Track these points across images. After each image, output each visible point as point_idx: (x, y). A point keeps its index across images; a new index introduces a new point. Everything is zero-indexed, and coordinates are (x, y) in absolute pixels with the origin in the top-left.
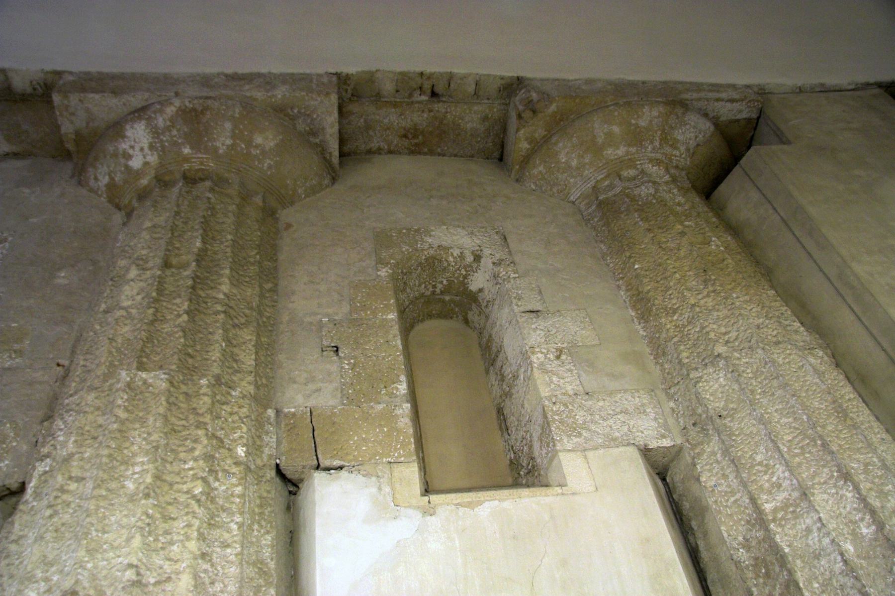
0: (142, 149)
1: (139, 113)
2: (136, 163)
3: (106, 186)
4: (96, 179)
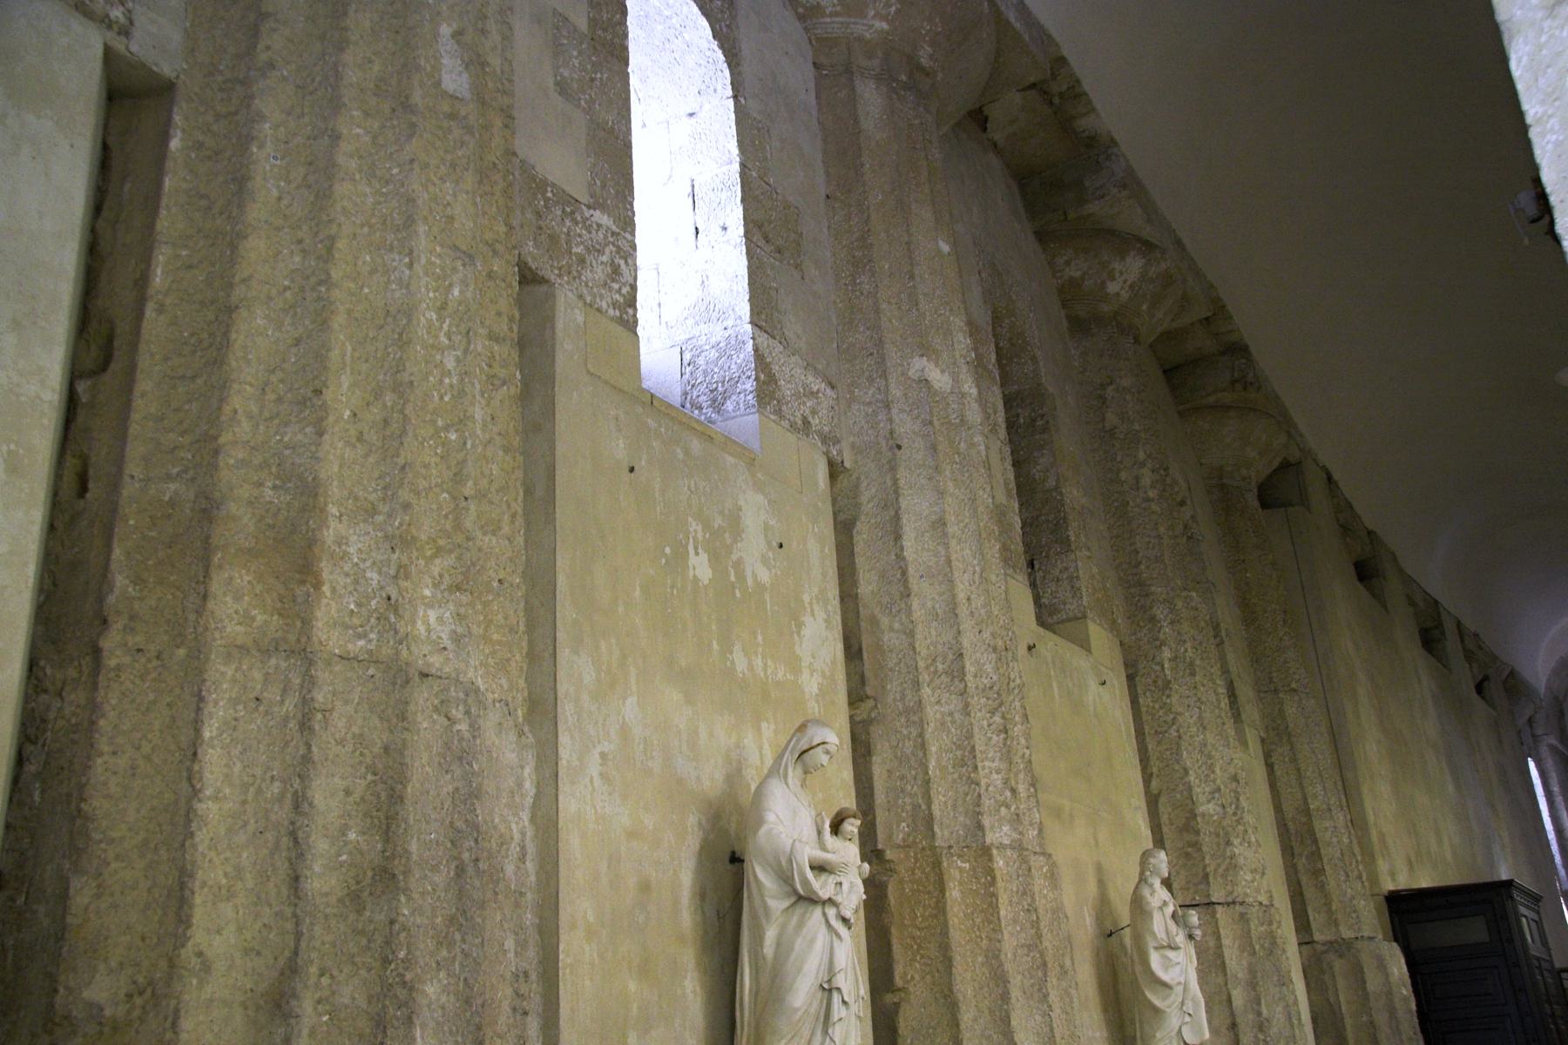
0: (1125, 281)
1: (1148, 247)
2: (1112, 288)
3: (1071, 277)
4: (1068, 263)
